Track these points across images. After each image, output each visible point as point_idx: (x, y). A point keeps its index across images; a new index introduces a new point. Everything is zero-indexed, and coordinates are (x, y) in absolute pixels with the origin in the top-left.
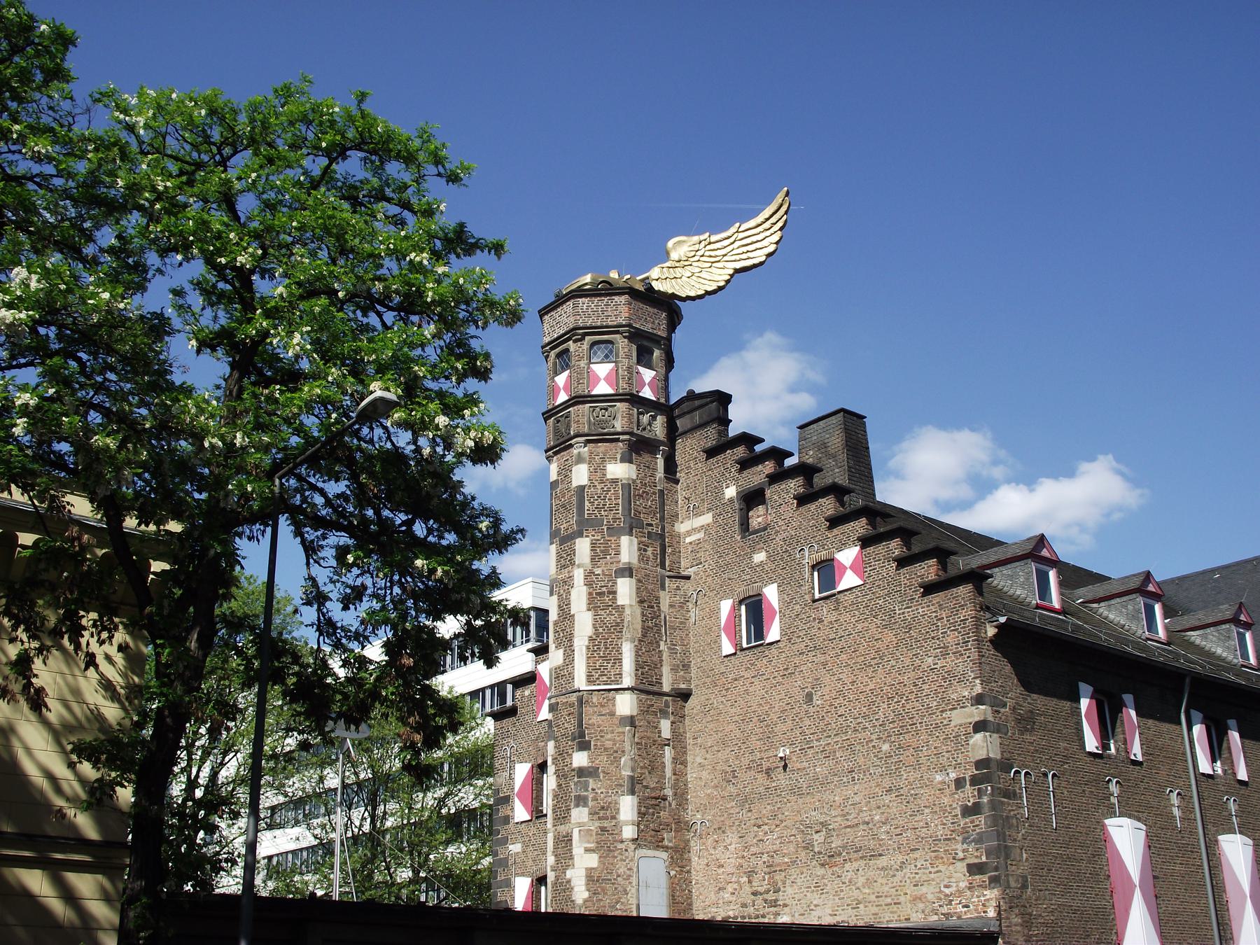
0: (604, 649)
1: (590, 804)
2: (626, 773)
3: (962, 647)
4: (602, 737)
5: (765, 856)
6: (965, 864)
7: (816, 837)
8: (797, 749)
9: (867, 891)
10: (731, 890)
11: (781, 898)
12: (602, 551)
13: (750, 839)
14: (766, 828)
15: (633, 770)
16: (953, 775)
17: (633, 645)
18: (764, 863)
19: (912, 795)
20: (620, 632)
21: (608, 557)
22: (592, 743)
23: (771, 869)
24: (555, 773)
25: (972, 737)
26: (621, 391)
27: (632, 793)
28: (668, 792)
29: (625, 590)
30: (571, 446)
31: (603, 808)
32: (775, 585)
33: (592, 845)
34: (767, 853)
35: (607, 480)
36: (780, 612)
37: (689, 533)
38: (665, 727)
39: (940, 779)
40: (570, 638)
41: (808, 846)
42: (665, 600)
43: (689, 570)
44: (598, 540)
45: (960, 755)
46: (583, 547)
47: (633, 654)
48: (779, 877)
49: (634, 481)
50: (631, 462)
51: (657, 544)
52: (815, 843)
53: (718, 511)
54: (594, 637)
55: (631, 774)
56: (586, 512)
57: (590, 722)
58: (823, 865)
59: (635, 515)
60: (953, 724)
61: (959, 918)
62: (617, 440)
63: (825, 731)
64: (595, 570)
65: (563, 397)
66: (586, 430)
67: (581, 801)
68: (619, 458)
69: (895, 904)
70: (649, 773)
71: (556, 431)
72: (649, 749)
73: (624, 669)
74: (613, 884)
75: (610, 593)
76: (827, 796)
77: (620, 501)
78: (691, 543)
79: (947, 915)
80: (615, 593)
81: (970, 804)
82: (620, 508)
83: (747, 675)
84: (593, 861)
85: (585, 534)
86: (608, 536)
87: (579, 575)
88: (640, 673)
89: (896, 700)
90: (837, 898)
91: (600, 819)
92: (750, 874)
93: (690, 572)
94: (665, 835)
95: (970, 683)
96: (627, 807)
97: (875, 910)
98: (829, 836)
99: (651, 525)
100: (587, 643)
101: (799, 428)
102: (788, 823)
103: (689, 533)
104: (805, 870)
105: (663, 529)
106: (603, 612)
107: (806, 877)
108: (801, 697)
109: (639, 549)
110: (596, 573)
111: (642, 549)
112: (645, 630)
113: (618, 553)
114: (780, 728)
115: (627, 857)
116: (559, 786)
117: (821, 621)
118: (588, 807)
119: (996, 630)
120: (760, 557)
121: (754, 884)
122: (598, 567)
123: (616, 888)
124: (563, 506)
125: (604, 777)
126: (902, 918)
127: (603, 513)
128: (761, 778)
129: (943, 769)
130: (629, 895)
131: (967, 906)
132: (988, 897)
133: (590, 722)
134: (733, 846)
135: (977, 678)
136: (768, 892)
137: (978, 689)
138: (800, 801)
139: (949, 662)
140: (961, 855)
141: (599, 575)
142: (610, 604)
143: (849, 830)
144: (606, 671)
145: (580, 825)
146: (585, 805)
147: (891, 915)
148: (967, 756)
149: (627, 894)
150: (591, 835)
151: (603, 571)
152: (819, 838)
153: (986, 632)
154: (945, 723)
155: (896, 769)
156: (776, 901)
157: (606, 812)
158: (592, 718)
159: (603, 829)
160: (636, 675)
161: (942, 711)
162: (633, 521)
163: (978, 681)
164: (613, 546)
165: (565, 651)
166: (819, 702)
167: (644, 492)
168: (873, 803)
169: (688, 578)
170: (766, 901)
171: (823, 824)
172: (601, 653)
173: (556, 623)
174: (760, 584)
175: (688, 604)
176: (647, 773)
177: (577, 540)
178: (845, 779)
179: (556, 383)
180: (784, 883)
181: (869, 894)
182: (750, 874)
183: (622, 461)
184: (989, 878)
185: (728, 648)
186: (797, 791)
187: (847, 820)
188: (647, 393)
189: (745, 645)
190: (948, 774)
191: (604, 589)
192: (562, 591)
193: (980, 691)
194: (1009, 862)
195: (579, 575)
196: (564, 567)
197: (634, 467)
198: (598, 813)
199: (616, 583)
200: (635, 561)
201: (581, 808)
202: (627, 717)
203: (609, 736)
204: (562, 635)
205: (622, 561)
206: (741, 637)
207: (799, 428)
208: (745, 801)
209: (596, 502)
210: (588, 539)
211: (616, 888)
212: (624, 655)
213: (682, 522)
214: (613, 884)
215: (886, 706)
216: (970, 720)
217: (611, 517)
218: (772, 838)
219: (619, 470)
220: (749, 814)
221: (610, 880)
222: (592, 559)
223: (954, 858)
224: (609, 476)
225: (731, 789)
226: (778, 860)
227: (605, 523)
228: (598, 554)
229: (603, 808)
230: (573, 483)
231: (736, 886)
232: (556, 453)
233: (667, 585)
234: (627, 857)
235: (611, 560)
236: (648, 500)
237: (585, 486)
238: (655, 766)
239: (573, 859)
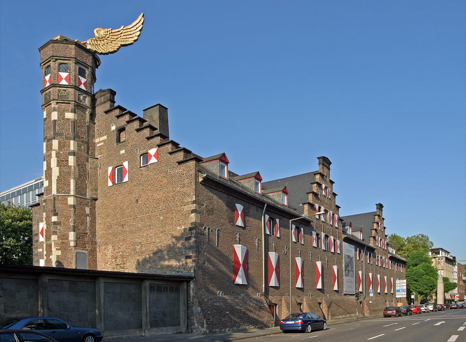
0: (62, 181)
1: (58, 234)
2: (72, 224)
3: (190, 184)
4: (62, 211)
5: (121, 253)
6: (185, 256)
7: (137, 247)
8: (132, 218)
9: (153, 264)
10: (109, 264)
12: (63, 145)
14: (121, 244)
15: (74, 223)
16: (183, 227)
17: (75, 180)
18: (120, 255)
19: (169, 234)
20: (70, 175)
21: (65, 148)
22: (59, 213)
24: (46, 224)
25: (191, 215)
27: (74, 231)
28: (88, 231)
29: (71, 160)
30: (51, 104)
31: (63, 236)
32: (127, 161)
33: (59, 248)
34: (121, 252)
35: (66, 118)
36: (128, 171)
37: (98, 143)
38: (87, 210)
39: (179, 228)
40: (51, 176)
41: (135, 249)
42: (89, 166)
43: (98, 156)
44: (61, 141)
45: (186, 221)
46: (55, 143)
47: (75, 184)
48: (125, 260)
49: (76, 121)
50: (75, 113)
52: (137, 249)
53: (109, 135)
54: (60, 176)
55: (74, 225)
56: (57, 130)
57: (58, 206)
58: (139, 256)
59: (76, 133)
60: (184, 210)
61: (182, 272)
63: (142, 212)
65: (48, 84)
66: (57, 98)
67: (55, 233)
68: (70, 111)
69: (162, 268)
70: (81, 225)
71: (46, 98)
72: (79, 216)
73: (71, 188)
74: (67, 260)
75: (66, 161)
76: (141, 234)
78: (99, 146)
79: (178, 272)
80: (68, 161)
81: (188, 237)
82: (70, 130)
84: (59, 253)
85: (56, 138)
86: (65, 140)
87: (54, 153)
88: (77, 190)
89: (166, 202)
90: (143, 266)
91: (62, 239)
93: (99, 157)
94: (87, 246)
95: (191, 196)
96: (72, 236)
97: (155, 270)
98: (141, 247)
99: (83, 138)
100: (57, 178)
101: (143, 111)
103: (98, 143)
104: (133, 257)
105: (88, 140)
106: (63, 168)
107: (133, 260)
108: (134, 201)
111: (79, 146)
112: (80, 176)
113: (69, 147)
114: (127, 211)
115: (72, 252)
116: (47, 228)
117: (142, 175)
118: (57, 235)
119: (202, 179)
120: (123, 152)
121: (117, 262)
123: (68, 262)
124: (48, 128)
125: (63, 225)
126: (164, 272)
128: (120, 228)
129: (180, 225)
130: (72, 264)
131: (185, 269)
132: (191, 266)
133: (58, 206)
134: (110, 249)
135: (194, 195)
137: (194, 199)
138: (133, 235)
139: (185, 190)
140: (184, 253)
141: (62, 154)
142: (66, 165)
143: (148, 245)
144: (64, 189)
145: (54, 241)
146: (56, 234)
147: (160, 272)
148: (188, 221)
149: (72, 264)
150: (59, 244)
151: (63, 153)
152: (138, 247)
153: (199, 180)
154: (182, 210)
155: (165, 225)
156: (124, 267)
157: (64, 237)
158: (59, 205)
159: (63, 243)
160: (76, 191)
161: (181, 206)
162: (76, 135)
163: (194, 196)
165: (49, 181)
166: (140, 203)
167: (80, 125)
168: (156, 236)
169: (98, 159)
170: (120, 267)
171: (140, 243)
172: (62, 182)
173: (46, 171)
174: (122, 161)
175: (97, 168)
176: (80, 225)
177: (53, 140)
178: (148, 228)
179: (45, 79)
181: (153, 265)
183: (71, 112)
184: (193, 260)
185: (110, 184)
186: (131, 232)
187: (148, 241)
188: (82, 87)
189: (116, 183)
190: (182, 227)
191: (63, 159)
192: (48, 159)
193: (194, 199)
194: (199, 255)
195: (54, 153)
196: (48, 150)
197: (77, 115)
198: (61, 237)
199: (68, 157)
200: (76, 150)
201: (54, 235)
202: (72, 205)
203: (65, 211)
204: (48, 175)
205: (71, 150)
206: (115, 180)
207: (143, 111)
208: (114, 235)
209: (61, 127)
210: (57, 140)
211: (68, 262)
212: (71, 184)
213: (96, 139)
214: (67, 260)
215: (163, 204)
216: (190, 209)
217: (67, 133)
219: (70, 115)
220: (116, 239)
221: (66, 259)
222: (59, 148)
223: (181, 254)
224: (66, 117)
225: (110, 231)
227: (64, 135)
228: (61, 146)
229: (63, 236)
230: (52, 118)
231: (111, 262)
232: (45, 107)
233: (89, 161)
234: (72, 252)
236: (82, 128)
238: (83, 223)
239: (52, 252)
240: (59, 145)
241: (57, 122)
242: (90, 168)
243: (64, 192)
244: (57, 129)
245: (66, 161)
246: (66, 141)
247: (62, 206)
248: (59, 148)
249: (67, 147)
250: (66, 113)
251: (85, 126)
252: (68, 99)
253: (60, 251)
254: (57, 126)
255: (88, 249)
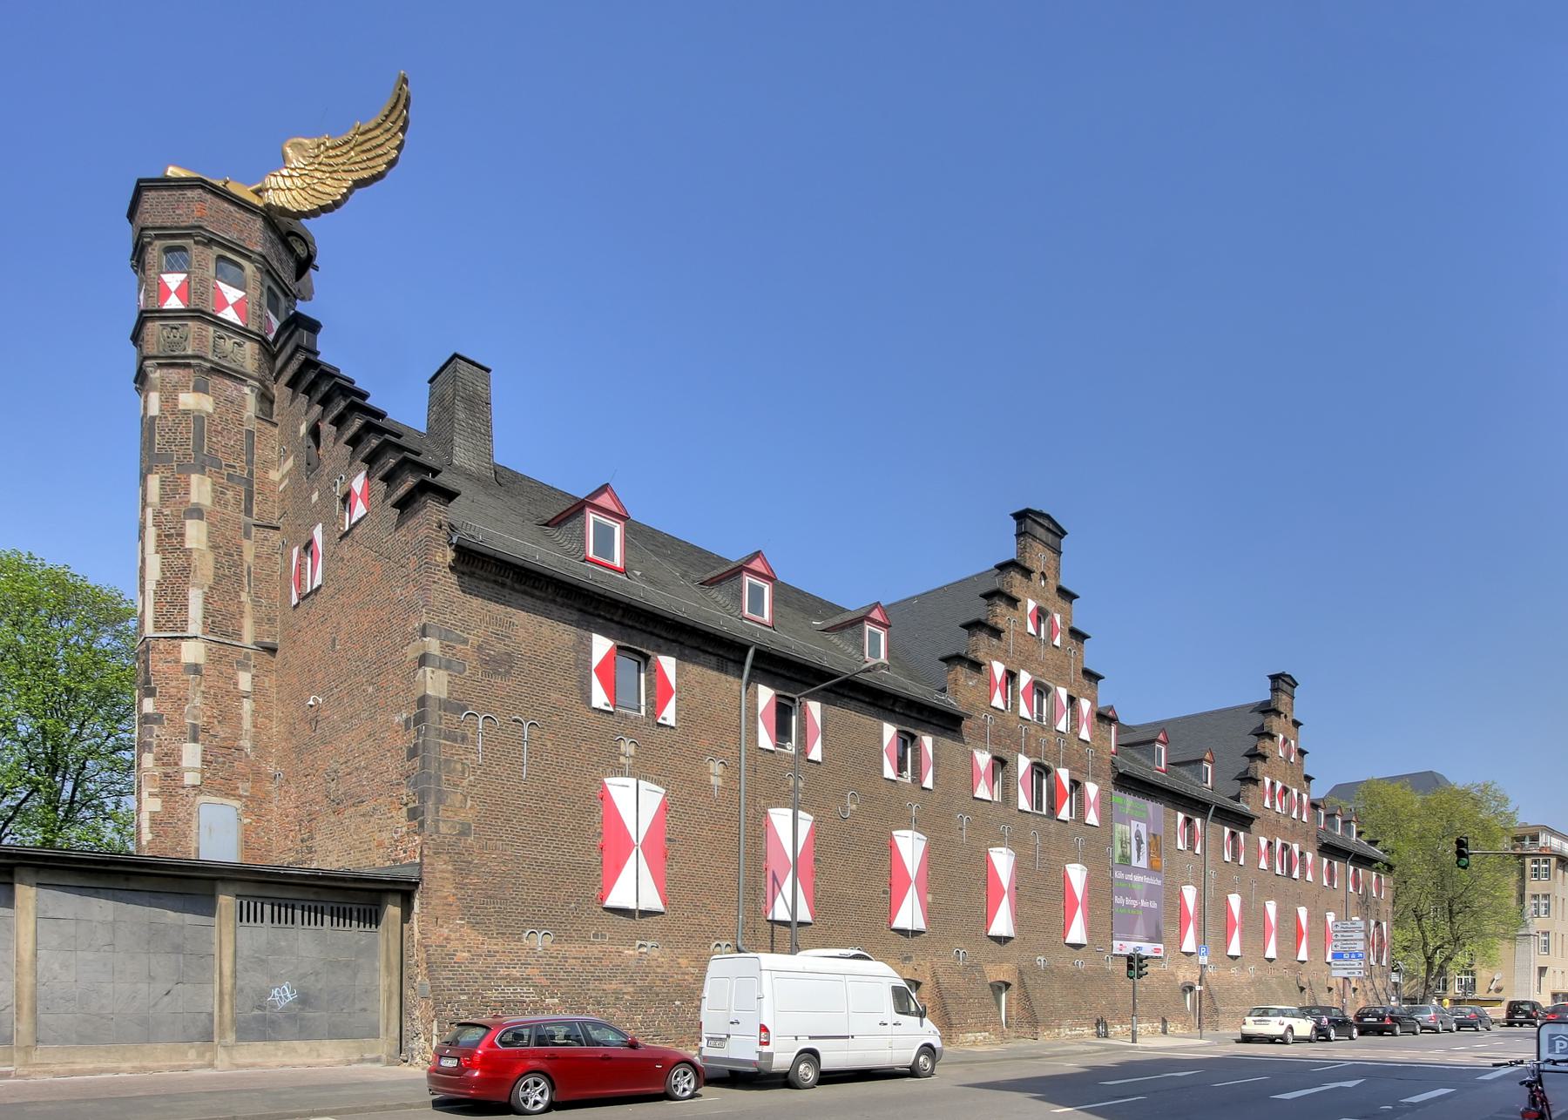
1: (155, 750)
21: (177, 496)
22: (158, 690)
26: (193, 307)
29: (196, 534)
35: (179, 411)
44: (168, 478)
51: (242, 489)
54: (162, 581)
57: (156, 669)
59: (209, 452)
62: (188, 365)
64: (164, 510)
68: (191, 387)
74: (174, 827)
75: (178, 535)
77: (191, 435)
82: (191, 443)
85: (155, 471)
91: (163, 764)
96: (191, 755)
100: (154, 588)
109: (214, 491)
110: (166, 513)
122: (167, 507)
125: (168, 724)
127: (173, 448)
141: (167, 515)
142: (178, 547)
146: (150, 751)
149: (186, 837)
151: (172, 511)
157: (170, 759)
159: (167, 775)
162: (206, 458)
164: (182, 484)
167: (223, 429)
176: (216, 723)
191: (172, 531)
197: (211, 399)
198: (162, 760)
203: (174, 683)
209: (167, 435)
210: (157, 476)
211: (177, 832)
214: (174, 827)
221: (171, 823)
224: (181, 407)
227: (175, 459)
235: (180, 500)
237: (156, 416)
240: (161, 488)
241: (157, 422)
242: (257, 556)
243: (171, 626)
244: (158, 444)
245: (178, 535)
246: (178, 476)
247: (166, 669)
248: (161, 498)
249: (182, 495)
250: (180, 395)
251: (239, 432)
252: (183, 353)
253: (158, 801)
254: (157, 435)
255: (240, 796)
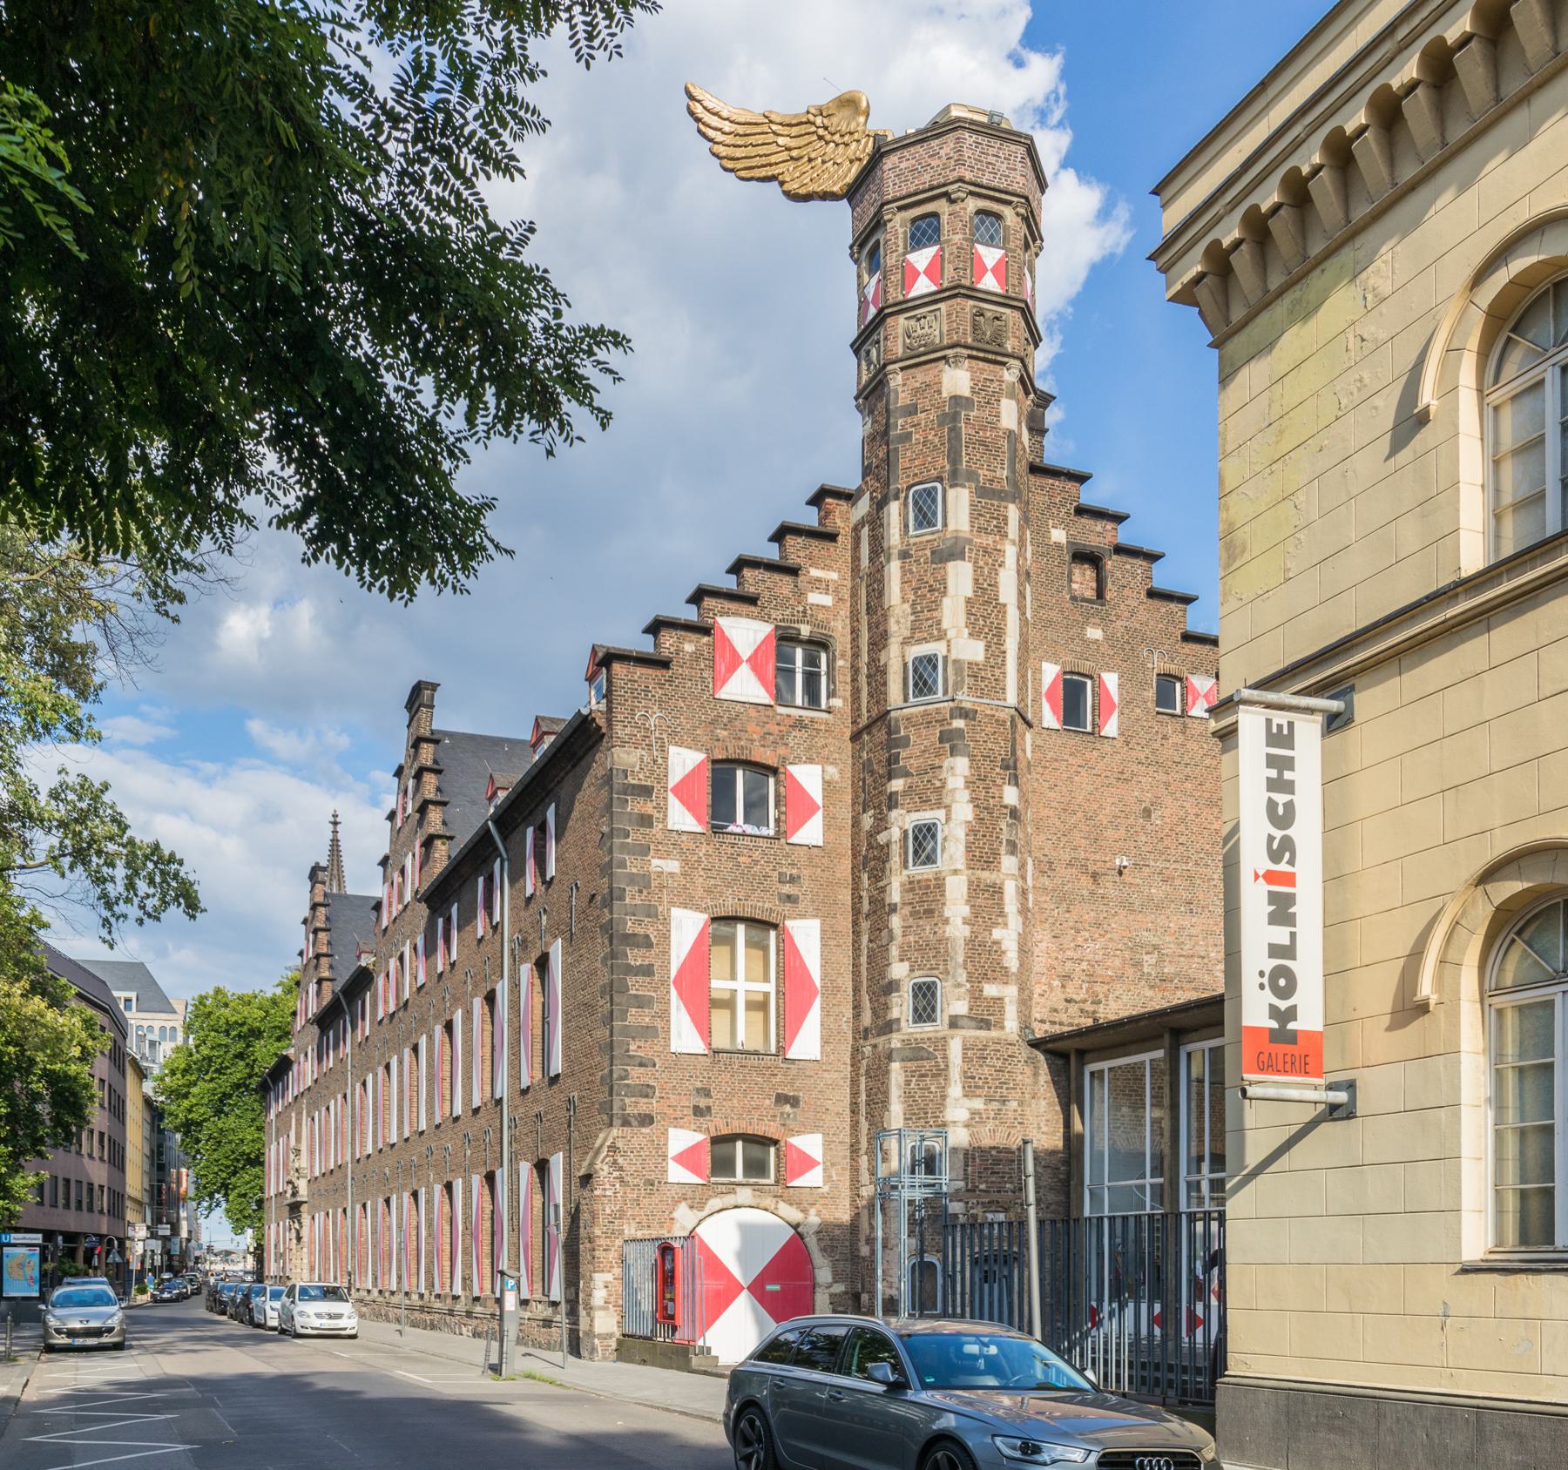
5: (1084, 965)
11: (1101, 1010)
13: (1067, 941)
23: (1091, 978)
41: (1138, 964)
58: (1152, 987)
83: (1071, 760)
92: (1066, 977)
102: (1115, 936)
128: (1086, 881)
136: (1085, 1001)
143: (1182, 959)
152: (1149, 960)
180: (1106, 996)
182: (1066, 977)
208: (1064, 898)
218: (1093, 949)
220: (1067, 915)
226: (1099, 970)
